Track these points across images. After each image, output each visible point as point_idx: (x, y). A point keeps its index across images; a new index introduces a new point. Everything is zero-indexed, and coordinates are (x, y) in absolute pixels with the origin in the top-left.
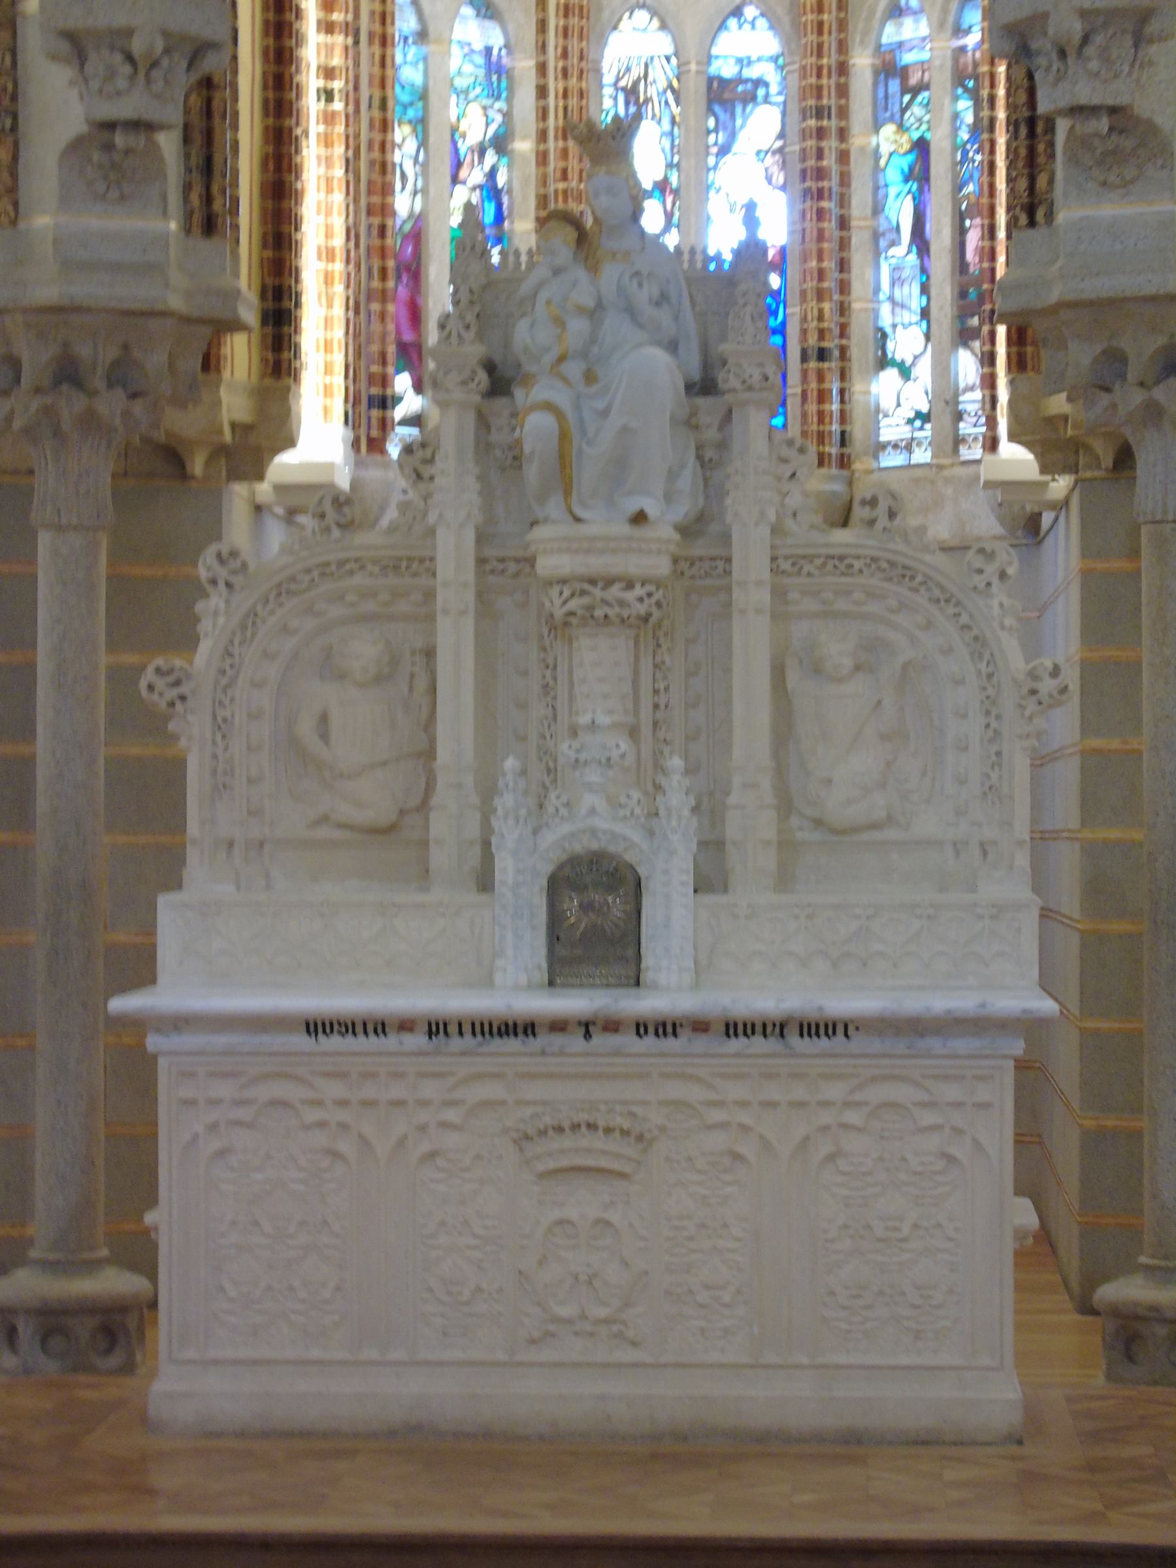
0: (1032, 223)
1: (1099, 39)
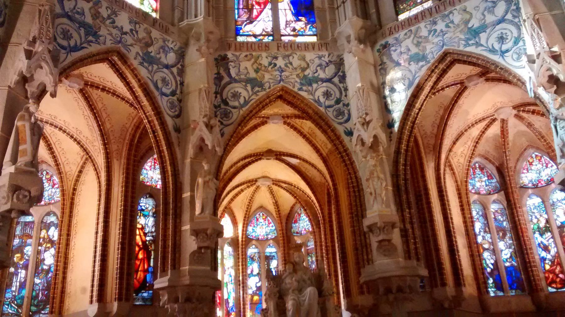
0: (369, 264)
1: (386, 228)
